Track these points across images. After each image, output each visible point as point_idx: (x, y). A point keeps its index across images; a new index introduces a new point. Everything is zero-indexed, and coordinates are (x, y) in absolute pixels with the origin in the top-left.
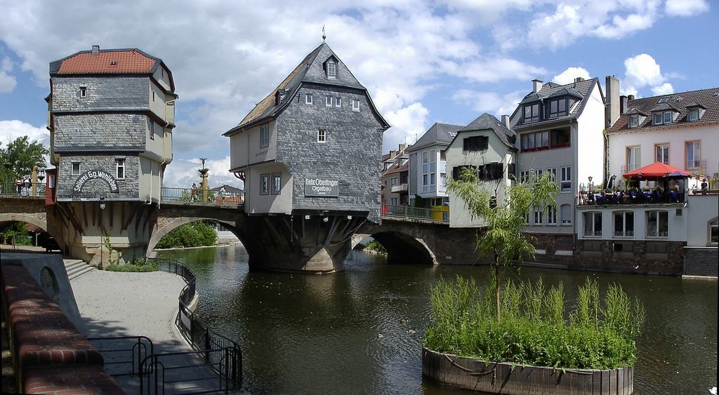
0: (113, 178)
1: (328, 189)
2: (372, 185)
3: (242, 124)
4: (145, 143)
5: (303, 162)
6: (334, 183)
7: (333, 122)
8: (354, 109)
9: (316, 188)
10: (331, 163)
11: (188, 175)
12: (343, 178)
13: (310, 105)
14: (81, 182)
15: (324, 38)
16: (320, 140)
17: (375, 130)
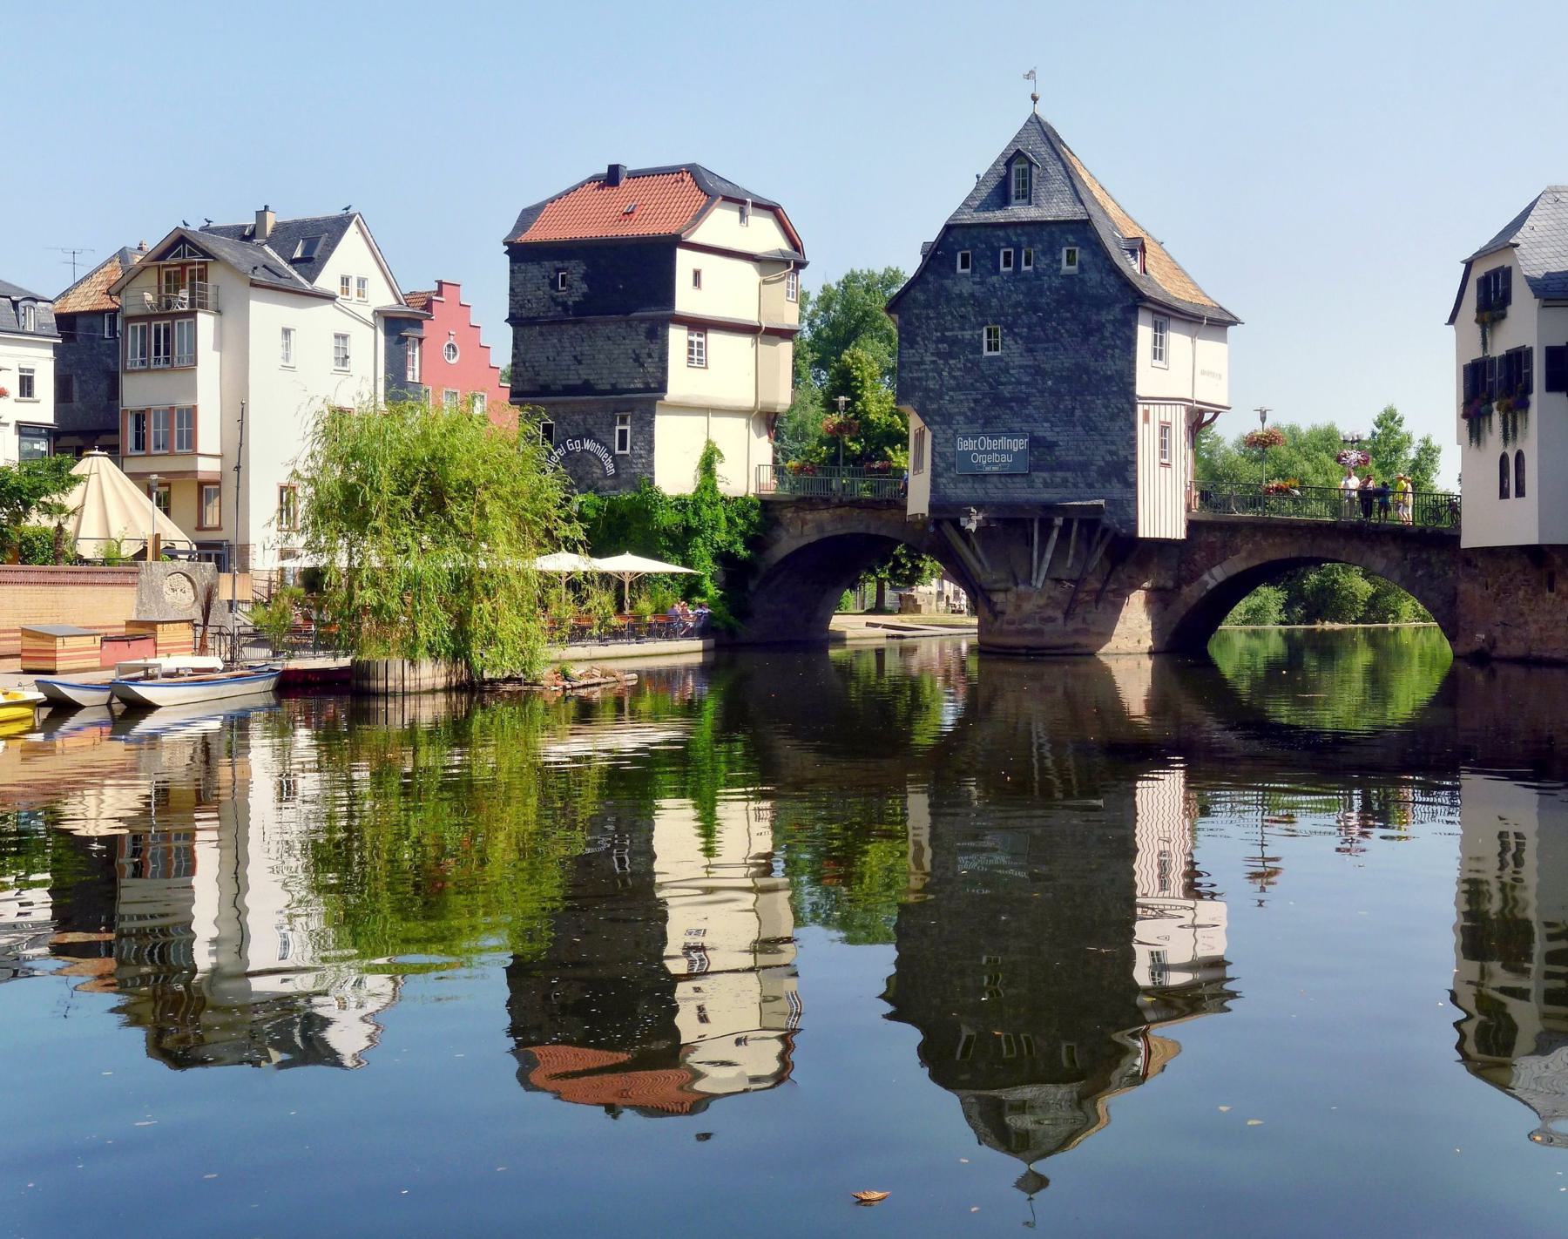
0: (610, 452)
1: (1005, 458)
2: (1113, 443)
5: (951, 401)
6: (1020, 444)
8: (1065, 268)
9: (979, 457)
10: (1012, 400)
11: (1062, 440)
12: (1044, 431)
13: (964, 275)
15: (1035, 99)
17: (1117, 312)
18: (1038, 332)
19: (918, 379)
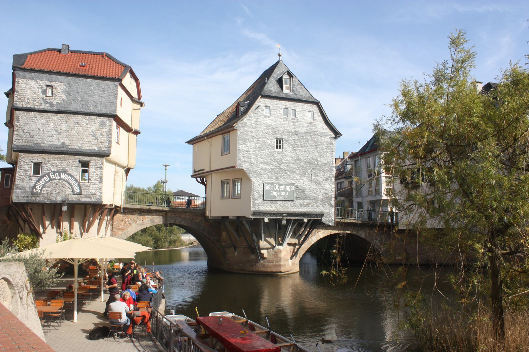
0: (76, 180)
3: (204, 133)
4: (110, 147)
5: (262, 168)
7: (289, 132)
9: (274, 193)
10: (287, 170)
12: (299, 183)
14: (42, 183)
16: (277, 148)
18: (298, 143)
19: (248, 158)
